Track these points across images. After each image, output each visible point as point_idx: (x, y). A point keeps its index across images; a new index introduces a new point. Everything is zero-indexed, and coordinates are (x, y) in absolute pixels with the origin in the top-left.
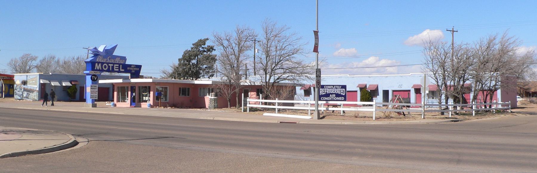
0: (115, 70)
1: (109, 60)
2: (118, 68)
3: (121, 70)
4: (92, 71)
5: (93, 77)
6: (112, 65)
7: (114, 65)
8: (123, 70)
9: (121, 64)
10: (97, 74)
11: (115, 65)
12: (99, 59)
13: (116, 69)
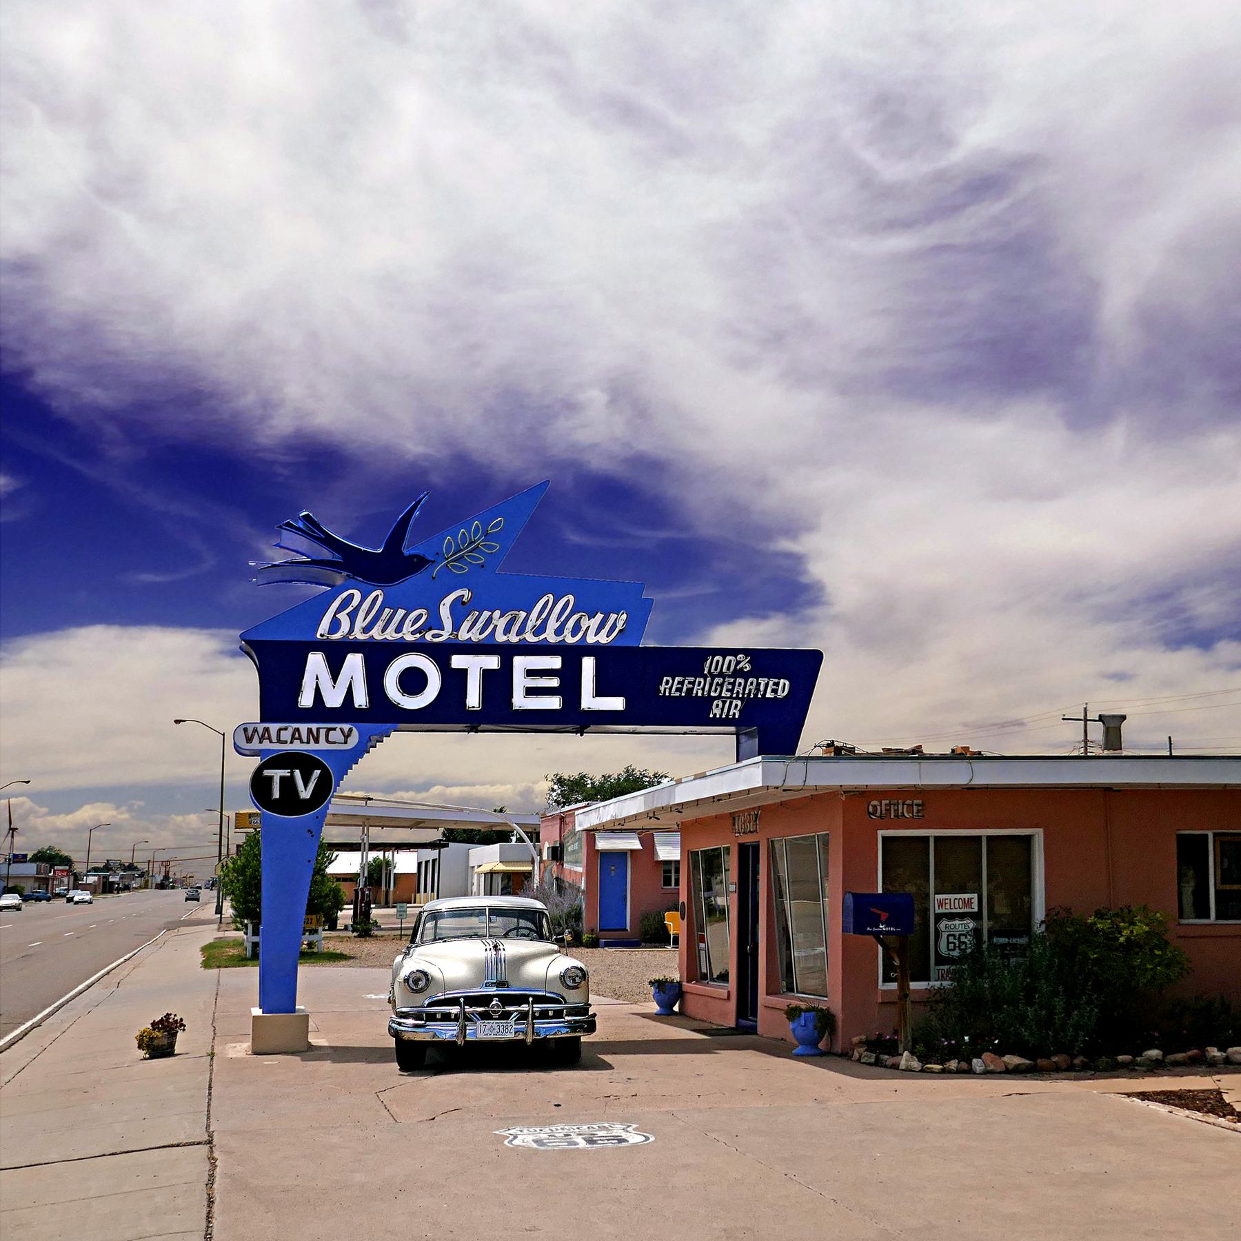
0: (520, 701)
1: (458, 617)
2: (554, 682)
3: (590, 701)
4: (274, 727)
5: (277, 774)
6: (492, 662)
7: (507, 667)
8: (616, 703)
9: (592, 649)
10: (323, 745)
11: (521, 663)
12: (343, 617)
13: (530, 692)
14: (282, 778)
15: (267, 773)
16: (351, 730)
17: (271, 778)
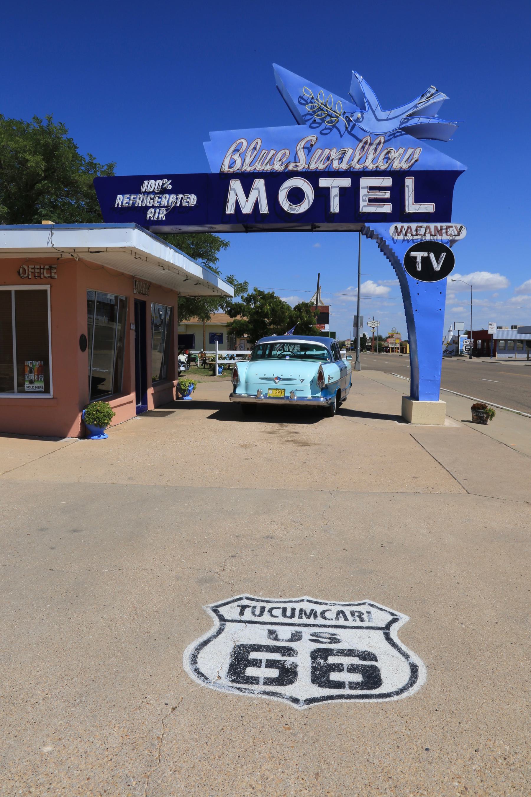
5: (419, 255)
14: (423, 258)
15: (413, 254)
16: (461, 227)
17: (415, 258)
